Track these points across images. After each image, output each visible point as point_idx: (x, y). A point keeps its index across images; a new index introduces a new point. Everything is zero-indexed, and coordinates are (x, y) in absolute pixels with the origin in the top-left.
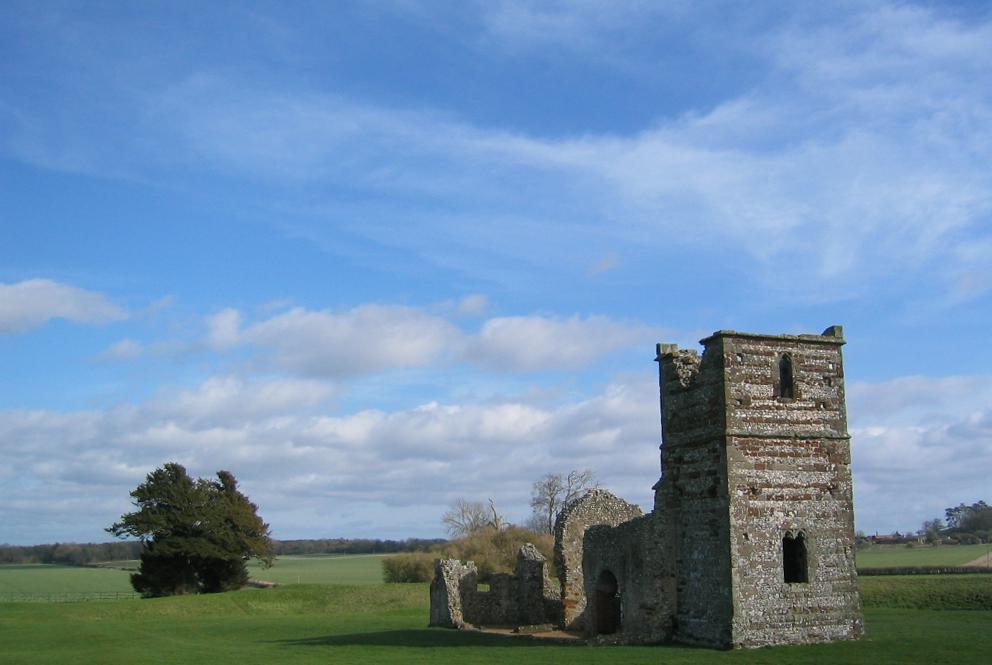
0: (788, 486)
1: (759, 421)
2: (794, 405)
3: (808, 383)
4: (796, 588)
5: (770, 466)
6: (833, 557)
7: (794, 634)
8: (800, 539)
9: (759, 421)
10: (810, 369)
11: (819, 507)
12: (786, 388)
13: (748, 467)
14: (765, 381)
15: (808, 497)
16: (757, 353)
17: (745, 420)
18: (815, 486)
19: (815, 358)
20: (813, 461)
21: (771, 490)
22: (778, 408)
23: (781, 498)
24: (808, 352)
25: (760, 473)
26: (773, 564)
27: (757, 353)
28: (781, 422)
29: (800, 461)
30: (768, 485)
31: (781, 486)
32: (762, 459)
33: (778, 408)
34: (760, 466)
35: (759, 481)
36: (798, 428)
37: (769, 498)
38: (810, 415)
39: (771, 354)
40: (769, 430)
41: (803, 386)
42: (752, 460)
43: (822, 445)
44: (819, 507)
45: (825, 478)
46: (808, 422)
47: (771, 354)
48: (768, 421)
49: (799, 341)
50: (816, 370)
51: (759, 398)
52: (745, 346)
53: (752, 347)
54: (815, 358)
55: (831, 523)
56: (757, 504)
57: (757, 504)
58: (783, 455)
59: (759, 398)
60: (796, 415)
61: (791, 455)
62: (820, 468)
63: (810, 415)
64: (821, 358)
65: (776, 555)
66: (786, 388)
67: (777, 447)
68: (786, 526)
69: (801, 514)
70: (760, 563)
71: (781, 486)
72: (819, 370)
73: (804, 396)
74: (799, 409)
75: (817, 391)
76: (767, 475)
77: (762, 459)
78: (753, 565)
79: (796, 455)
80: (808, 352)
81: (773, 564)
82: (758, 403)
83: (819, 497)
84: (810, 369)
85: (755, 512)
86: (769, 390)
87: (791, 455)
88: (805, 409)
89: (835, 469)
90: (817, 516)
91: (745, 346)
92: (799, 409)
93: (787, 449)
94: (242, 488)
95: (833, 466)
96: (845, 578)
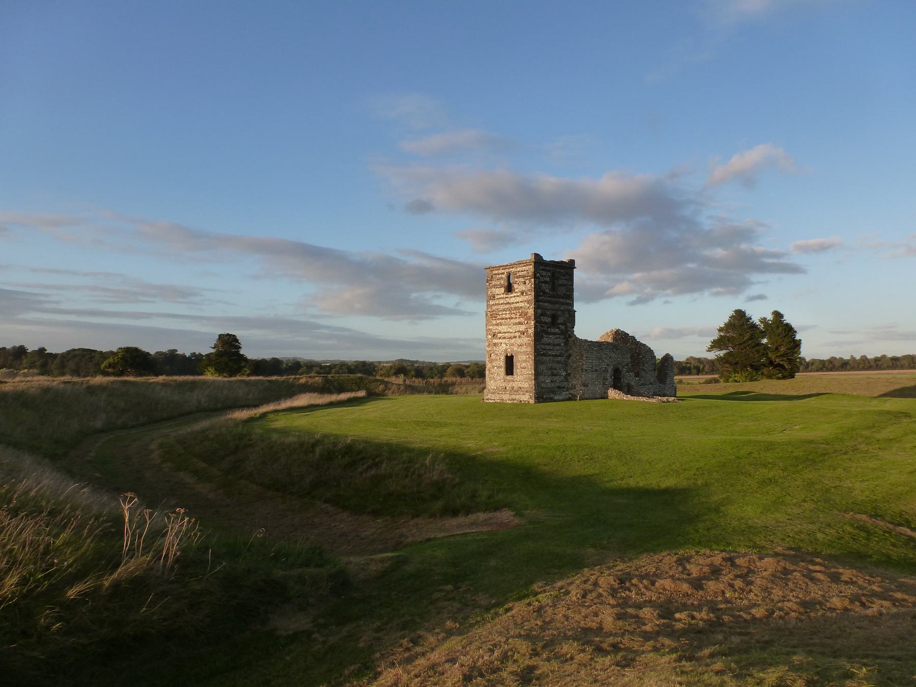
0: (508, 333)
1: (499, 304)
2: (512, 295)
3: (518, 284)
4: (509, 377)
5: (501, 324)
6: (524, 365)
7: (506, 397)
8: (512, 356)
9: (499, 304)
10: (520, 277)
11: (519, 341)
12: (509, 289)
13: (493, 325)
14: (501, 286)
15: (515, 337)
16: (498, 274)
17: (493, 305)
18: (519, 331)
19: (522, 271)
20: (517, 320)
21: (501, 335)
22: (506, 298)
23: (504, 338)
24: (519, 269)
25: (497, 327)
26: (500, 367)
27: (498, 274)
28: (508, 303)
29: (512, 321)
30: (500, 333)
31: (505, 333)
32: (498, 322)
33: (506, 298)
34: (497, 325)
35: (496, 331)
36: (512, 306)
37: (500, 338)
38: (518, 299)
39: (503, 273)
40: (501, 307)
41: (515, 286)
42: (494, 322)
43: (522, 312)
44: (519, 341)
45: (522, 328)
46: (518, 302)
47: (503, 273)
48: (502, 304)
49: (512, 266)
50: (522, 277)
51: (499, 294)
52: (494, 272)
53: (496, 272)
54: (522, 271)
55: (524, 349)
56: (495, 341)
57: (495, 341)
58: (506, 319)
59: (499, 294)
60: (512, 300)
61: (509, 318)
62: (520, 323)
63: (518, 299)
64: (525, 271)
65: (502, 363)
66: (509, 289)
67: (504, 316)
68: (506, 350)
69: (512, 345)
70: (496, 366)
71: (505, 333)
72: (523, 277)
73: (516, 291)
74: (515, 297)
75: (522, 287)
76: (500, 328)
77: (498, 322)
78: (493, 367)
79: (512, 318)
80: (519, 269)
81: (500, 367)
82: (498, 297)
83: (519, 337)
84: (520, 277)
85: (495, 344)
86: (503, 290)
87: (509, 318)
88: (517, 296)
89: (527, 323)
90: (519, 346)
91: (494, 272)
92: (515, 297)
93: (508, 316)
94: (788, 319)
95: (526, 322)
96: (529, 374)
